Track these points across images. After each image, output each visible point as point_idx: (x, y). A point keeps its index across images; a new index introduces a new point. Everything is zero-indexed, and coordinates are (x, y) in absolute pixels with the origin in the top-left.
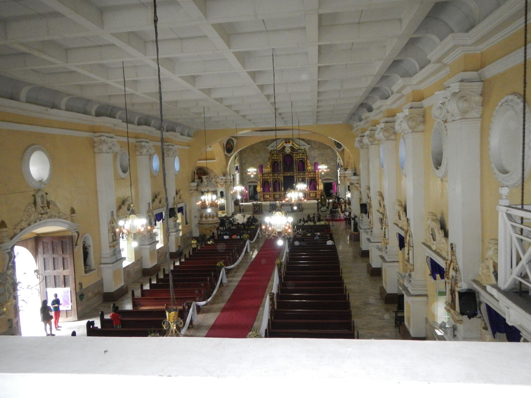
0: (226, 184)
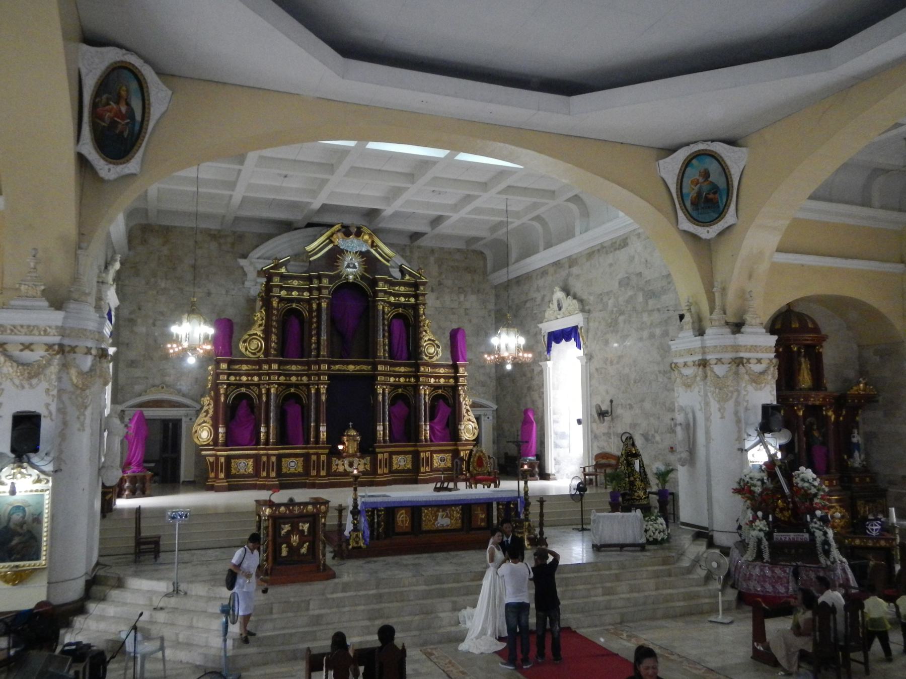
0: (65, 366)
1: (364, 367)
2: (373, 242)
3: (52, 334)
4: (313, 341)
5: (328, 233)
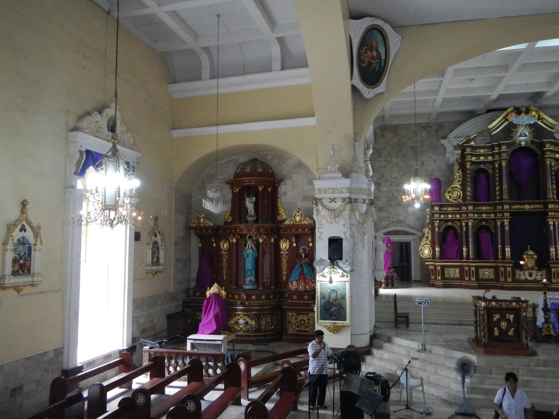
0: (352, 210)
1: (538, 206)
2: (539, 116)
3: (344, 192)
4: (497, 189)
5: (504, 114)
